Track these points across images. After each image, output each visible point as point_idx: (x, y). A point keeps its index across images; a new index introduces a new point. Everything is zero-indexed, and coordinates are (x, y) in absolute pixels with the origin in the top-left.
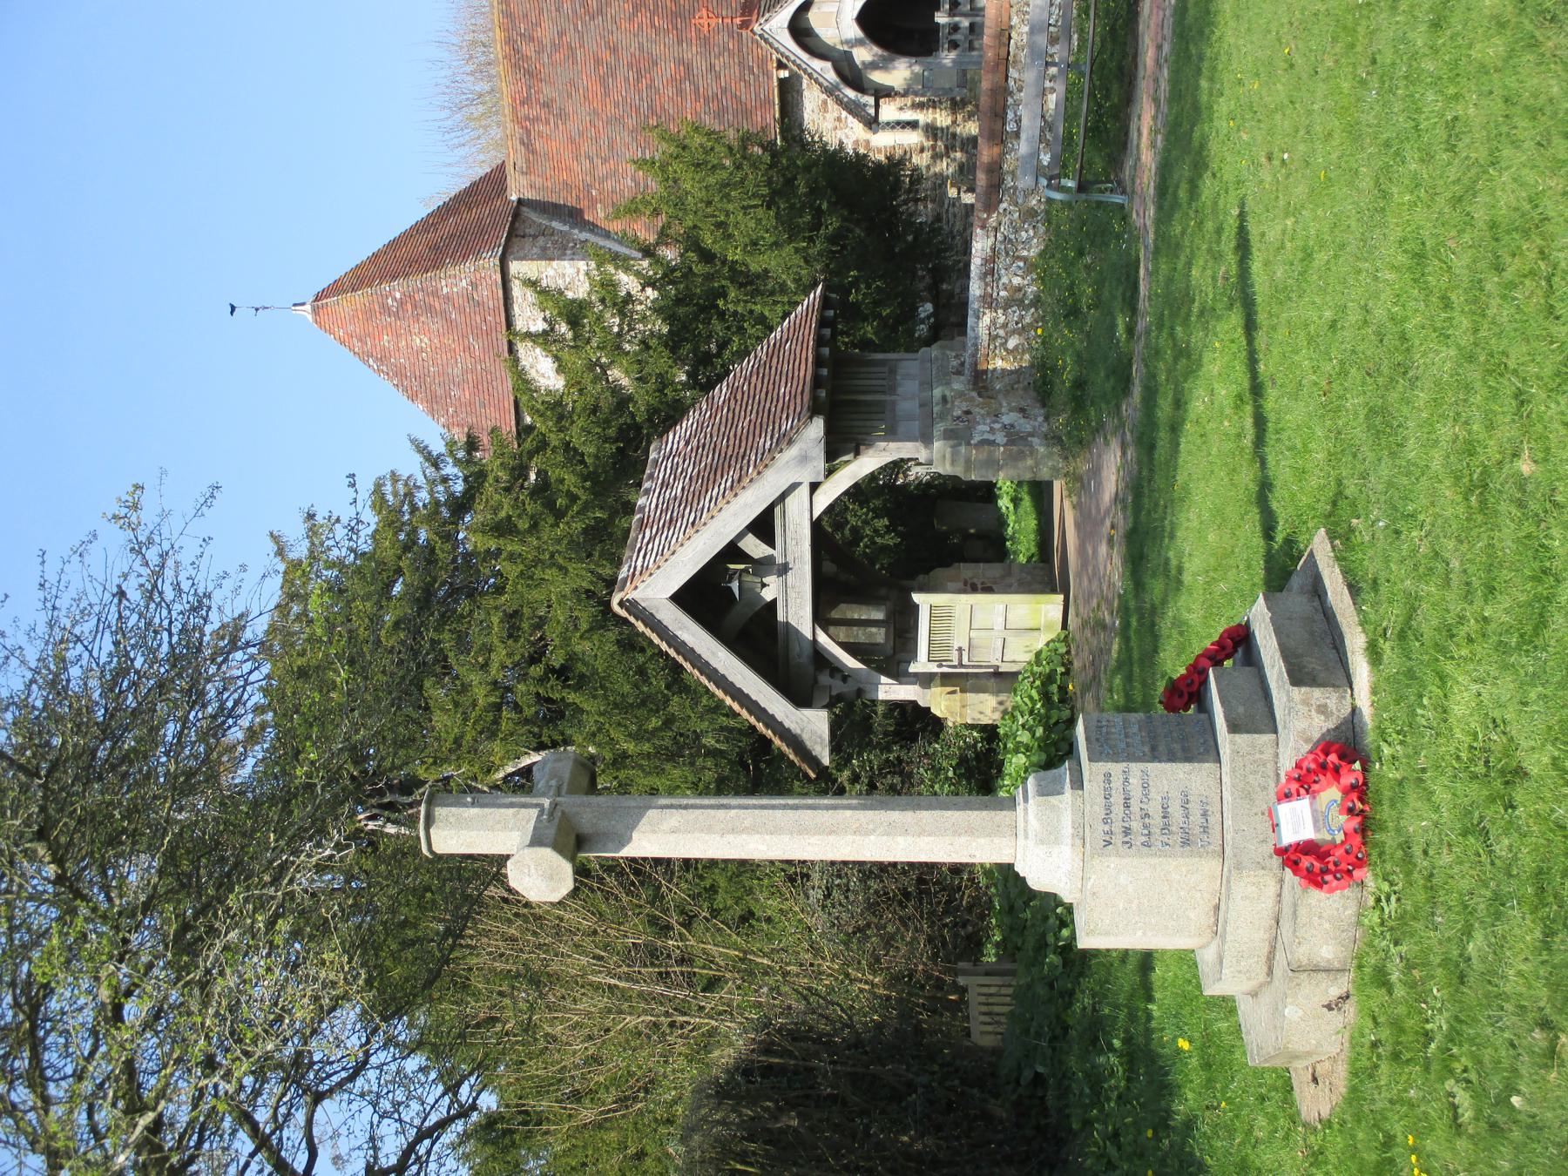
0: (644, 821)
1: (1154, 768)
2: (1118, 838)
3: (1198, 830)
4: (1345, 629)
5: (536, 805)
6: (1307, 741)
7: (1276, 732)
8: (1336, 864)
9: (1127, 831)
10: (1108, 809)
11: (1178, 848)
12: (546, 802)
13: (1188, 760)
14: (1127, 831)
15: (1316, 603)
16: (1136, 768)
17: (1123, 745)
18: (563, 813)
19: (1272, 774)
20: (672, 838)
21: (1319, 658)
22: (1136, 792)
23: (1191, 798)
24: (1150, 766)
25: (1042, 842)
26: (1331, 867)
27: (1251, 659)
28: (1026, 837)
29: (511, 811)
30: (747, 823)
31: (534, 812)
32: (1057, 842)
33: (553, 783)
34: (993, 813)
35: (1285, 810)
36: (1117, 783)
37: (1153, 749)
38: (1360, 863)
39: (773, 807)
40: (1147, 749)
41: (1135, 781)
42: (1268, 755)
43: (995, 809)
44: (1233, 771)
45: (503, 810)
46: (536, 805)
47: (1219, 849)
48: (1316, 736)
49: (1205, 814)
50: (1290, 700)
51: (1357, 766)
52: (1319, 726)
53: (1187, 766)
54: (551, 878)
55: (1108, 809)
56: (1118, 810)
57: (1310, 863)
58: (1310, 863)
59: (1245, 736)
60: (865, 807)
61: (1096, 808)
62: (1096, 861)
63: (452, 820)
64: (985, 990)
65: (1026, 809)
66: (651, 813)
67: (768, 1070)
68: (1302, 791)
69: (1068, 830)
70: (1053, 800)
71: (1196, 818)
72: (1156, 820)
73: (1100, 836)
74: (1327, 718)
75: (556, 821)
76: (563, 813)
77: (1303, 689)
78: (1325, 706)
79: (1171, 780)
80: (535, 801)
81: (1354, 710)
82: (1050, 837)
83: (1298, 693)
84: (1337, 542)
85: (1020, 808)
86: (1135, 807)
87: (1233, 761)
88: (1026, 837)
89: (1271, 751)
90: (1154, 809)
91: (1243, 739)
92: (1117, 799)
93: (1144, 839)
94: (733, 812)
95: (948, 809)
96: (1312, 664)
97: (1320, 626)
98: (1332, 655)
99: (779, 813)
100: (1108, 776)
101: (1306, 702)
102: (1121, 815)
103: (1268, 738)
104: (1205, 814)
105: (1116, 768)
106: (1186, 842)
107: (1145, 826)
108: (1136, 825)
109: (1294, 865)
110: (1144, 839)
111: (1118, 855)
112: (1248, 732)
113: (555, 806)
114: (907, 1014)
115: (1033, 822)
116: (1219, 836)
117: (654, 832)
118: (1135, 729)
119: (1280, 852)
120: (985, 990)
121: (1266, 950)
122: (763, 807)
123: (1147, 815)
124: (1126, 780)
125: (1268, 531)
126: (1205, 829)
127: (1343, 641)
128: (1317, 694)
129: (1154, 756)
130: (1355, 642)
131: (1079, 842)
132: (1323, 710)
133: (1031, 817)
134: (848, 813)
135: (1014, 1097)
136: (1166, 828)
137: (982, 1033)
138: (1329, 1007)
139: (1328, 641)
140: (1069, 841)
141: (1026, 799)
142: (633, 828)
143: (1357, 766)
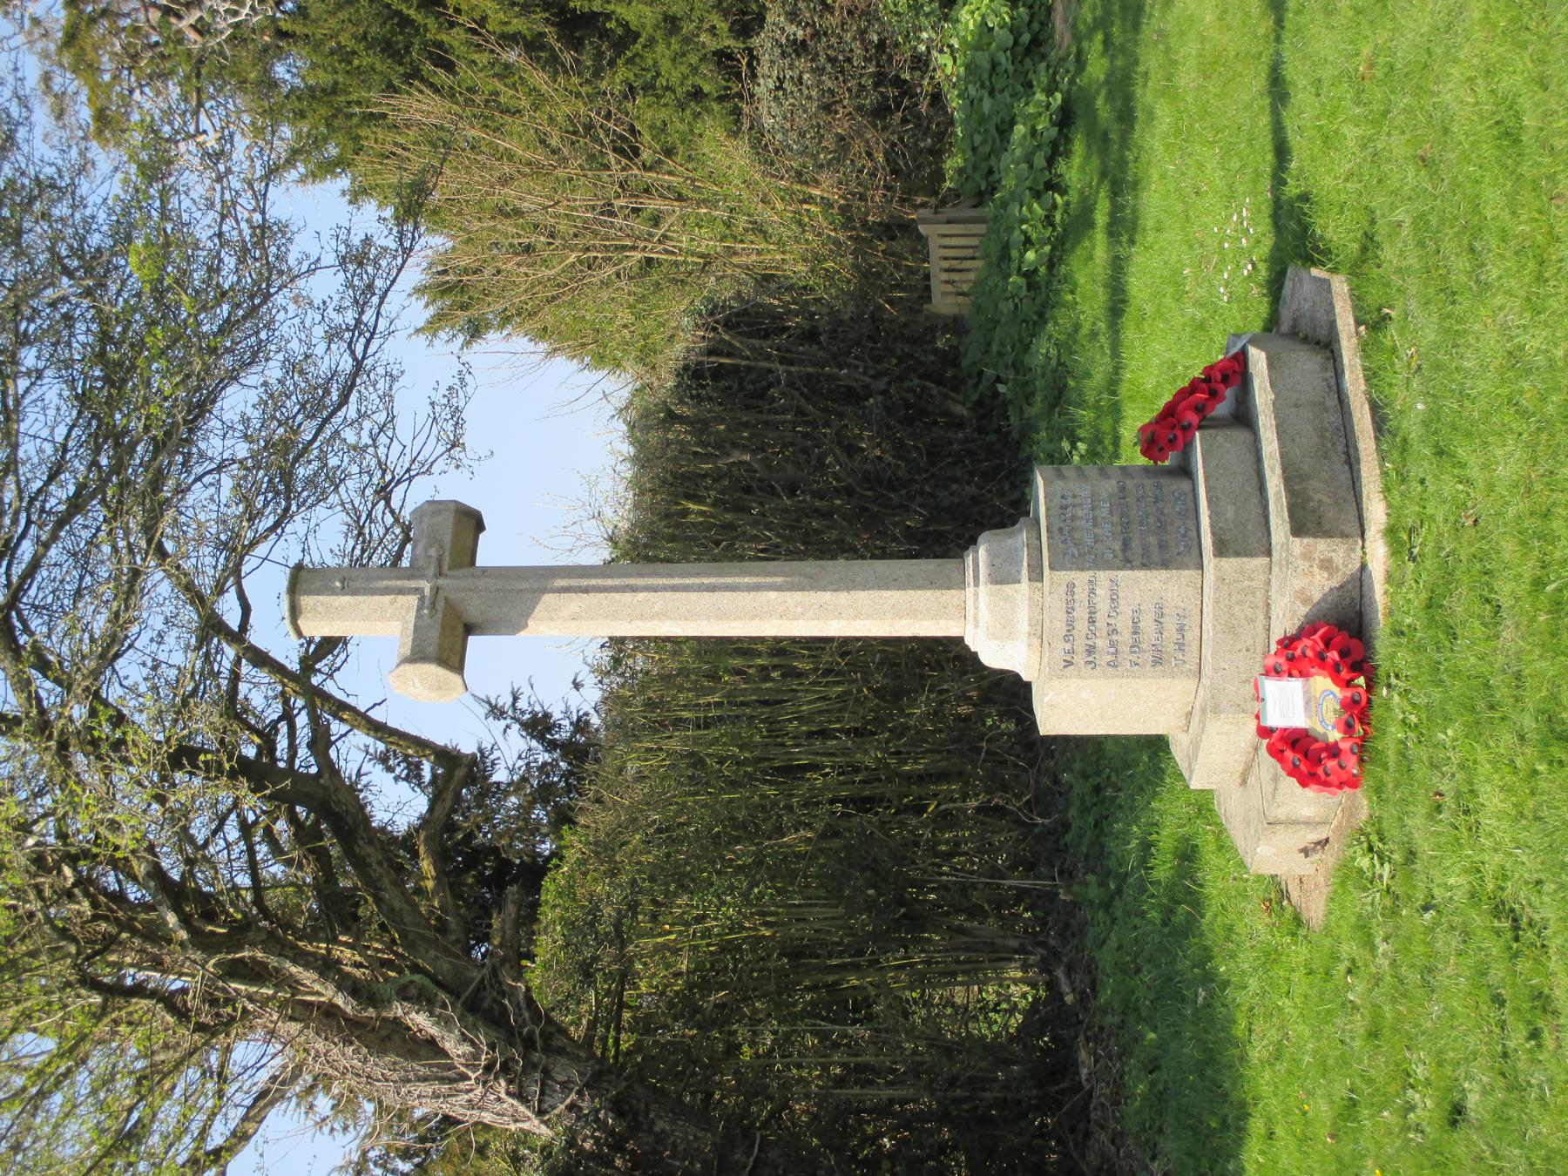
0: (539, 607)
1: (1124, 576)
2: (1080, 659)
3: (1171, 648)
4: (1362, 454)
5: (416, 590)
6: (1305, 602)
7: (1269, 554)
8: (1327, 774)
9: (1091, 650)
10: (1070, 625)
11: (1148, 667)
12: (427, 586)
13: (1165, 565)
14: (1091, 650)
15: (1331, 373)
16: (1103, 576)
17: (1089, 541)
18: (446, 599)
19: (1261, 605)
20: (574, 624)
21: (1323, 509)
22: (1103, 606)
23: (1166, 611)
24: (1121, 574)
25: (995, 637)
26: (1320, 771)
27: (1244, 418)
28: (976, 626)
29: (387, 598)
30: (656, 608)
31: (413, 600)
32: (1011, 636)
33: (433, 552)
34: (938, 593)
35: (1271, 686)
36: (1081, 594)
37: (1126, 546)
38: (1353, 783)
39: (686, 589)
40: (1117, 546)
41: (1102, 592)
42: (1258, 583)
43: (940, 588)
44: (1217, 602)
45: (377, 598)
46: (416, 590)
47: (1195, 668)
48: (1317, 596)
49: (1181, 630)
50: (1286, 547)
51: (1361, 681)
52: (1320, 585)
53: (1164, 574)
54: (440, 688)
55: (1070, 625)
56: (1081, 626)
57: (1299, 753)
58: (1299, 753)
59: (1234, 561)
60: (791, 588)
61: (1057, 624)
62: (1055, 682)
63: (321, 609)
64: (947, 241)
65: (976, 594)
66: (548, 598)
67: (718, 373)
68: (1295, 672)
69: (1024, 627)
70: (1008, 589)
71: (1171, 633)
72: (1125, 637)
73: (1059, 655)
74: (1331, 574)
75: (440, 615)
76: (446, 599)
77: (1306, 541)
78: (1330, 560)
79: (1145, 588)
80: (413, 584)
81: (1363, 567)
82: (1004, 630)
83: (1298, 545)
84: (1362, 328)
85: (970, 590)
86: (1101, 622)
87: (1217, 590)
88: (976, 626)
89: (1263, 577)
90: (1123, 623)
91: (1230, 564)
92: (1081, 613)
93: (1109, 658)
94: (641, 596)
95: (888, 588)
96: (1319, 494)
97: (1333, 418)
98: (1344, 476)
99: (693, 596)
100: (1071, 587)
101: (1307, 556)
102: (1085, 632)
103: (1261, 561)
104: (1181, 630)
105: (1080, 578)
106: (1158, 662)
107: (1112, 644)
108: (1101, 643)
109: (1275, 752)
110: (1109, 658)
111: (1079, 676)
112: (1237, 554)
113: (436, 590)
114: (861, 297)
115: (984, 614)
116: (1196, 654)
117: (552, 619)
118: (1103, 511)
119: (1264, 732)
120: (947, 241)
121: (1241, 769)
122: (675, 589)
123: (1115, 631)
124: (1092, 591)
125: (1278, 181)
126: (1181, 646)
127: (1358, 461)
128: (1322, 546)
129: (1127, 564)
130: (1376, 512)
131: (1036, 642)
132: (1327, 565)
133: (982, 606)
134: (773, 595)
135: (975, 397)
136: (1135, 645)
137: (943, 293)
138: (1306, 852)
139: (1341, 448)
140: (1024, 637)
141: (977, 584)
142: (528, 615)
143: (1361, 681)
